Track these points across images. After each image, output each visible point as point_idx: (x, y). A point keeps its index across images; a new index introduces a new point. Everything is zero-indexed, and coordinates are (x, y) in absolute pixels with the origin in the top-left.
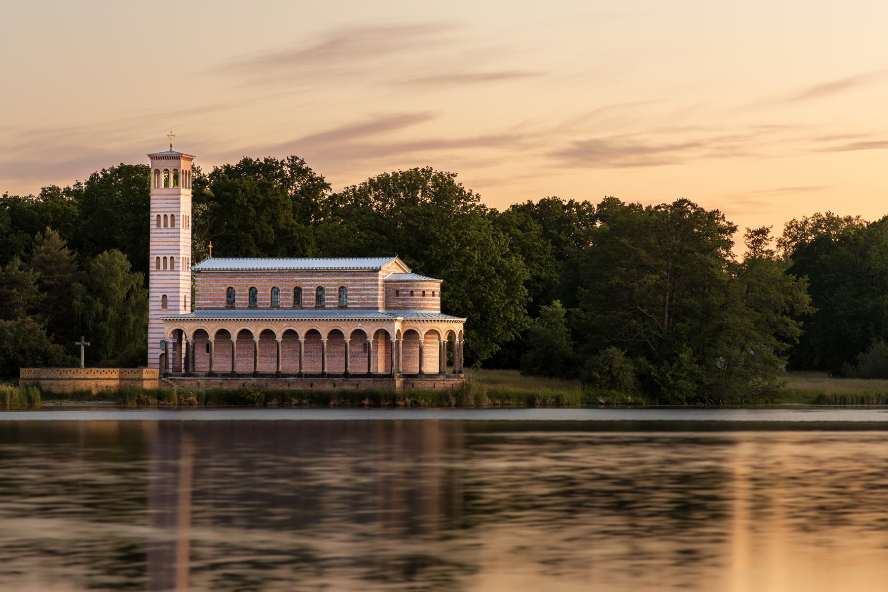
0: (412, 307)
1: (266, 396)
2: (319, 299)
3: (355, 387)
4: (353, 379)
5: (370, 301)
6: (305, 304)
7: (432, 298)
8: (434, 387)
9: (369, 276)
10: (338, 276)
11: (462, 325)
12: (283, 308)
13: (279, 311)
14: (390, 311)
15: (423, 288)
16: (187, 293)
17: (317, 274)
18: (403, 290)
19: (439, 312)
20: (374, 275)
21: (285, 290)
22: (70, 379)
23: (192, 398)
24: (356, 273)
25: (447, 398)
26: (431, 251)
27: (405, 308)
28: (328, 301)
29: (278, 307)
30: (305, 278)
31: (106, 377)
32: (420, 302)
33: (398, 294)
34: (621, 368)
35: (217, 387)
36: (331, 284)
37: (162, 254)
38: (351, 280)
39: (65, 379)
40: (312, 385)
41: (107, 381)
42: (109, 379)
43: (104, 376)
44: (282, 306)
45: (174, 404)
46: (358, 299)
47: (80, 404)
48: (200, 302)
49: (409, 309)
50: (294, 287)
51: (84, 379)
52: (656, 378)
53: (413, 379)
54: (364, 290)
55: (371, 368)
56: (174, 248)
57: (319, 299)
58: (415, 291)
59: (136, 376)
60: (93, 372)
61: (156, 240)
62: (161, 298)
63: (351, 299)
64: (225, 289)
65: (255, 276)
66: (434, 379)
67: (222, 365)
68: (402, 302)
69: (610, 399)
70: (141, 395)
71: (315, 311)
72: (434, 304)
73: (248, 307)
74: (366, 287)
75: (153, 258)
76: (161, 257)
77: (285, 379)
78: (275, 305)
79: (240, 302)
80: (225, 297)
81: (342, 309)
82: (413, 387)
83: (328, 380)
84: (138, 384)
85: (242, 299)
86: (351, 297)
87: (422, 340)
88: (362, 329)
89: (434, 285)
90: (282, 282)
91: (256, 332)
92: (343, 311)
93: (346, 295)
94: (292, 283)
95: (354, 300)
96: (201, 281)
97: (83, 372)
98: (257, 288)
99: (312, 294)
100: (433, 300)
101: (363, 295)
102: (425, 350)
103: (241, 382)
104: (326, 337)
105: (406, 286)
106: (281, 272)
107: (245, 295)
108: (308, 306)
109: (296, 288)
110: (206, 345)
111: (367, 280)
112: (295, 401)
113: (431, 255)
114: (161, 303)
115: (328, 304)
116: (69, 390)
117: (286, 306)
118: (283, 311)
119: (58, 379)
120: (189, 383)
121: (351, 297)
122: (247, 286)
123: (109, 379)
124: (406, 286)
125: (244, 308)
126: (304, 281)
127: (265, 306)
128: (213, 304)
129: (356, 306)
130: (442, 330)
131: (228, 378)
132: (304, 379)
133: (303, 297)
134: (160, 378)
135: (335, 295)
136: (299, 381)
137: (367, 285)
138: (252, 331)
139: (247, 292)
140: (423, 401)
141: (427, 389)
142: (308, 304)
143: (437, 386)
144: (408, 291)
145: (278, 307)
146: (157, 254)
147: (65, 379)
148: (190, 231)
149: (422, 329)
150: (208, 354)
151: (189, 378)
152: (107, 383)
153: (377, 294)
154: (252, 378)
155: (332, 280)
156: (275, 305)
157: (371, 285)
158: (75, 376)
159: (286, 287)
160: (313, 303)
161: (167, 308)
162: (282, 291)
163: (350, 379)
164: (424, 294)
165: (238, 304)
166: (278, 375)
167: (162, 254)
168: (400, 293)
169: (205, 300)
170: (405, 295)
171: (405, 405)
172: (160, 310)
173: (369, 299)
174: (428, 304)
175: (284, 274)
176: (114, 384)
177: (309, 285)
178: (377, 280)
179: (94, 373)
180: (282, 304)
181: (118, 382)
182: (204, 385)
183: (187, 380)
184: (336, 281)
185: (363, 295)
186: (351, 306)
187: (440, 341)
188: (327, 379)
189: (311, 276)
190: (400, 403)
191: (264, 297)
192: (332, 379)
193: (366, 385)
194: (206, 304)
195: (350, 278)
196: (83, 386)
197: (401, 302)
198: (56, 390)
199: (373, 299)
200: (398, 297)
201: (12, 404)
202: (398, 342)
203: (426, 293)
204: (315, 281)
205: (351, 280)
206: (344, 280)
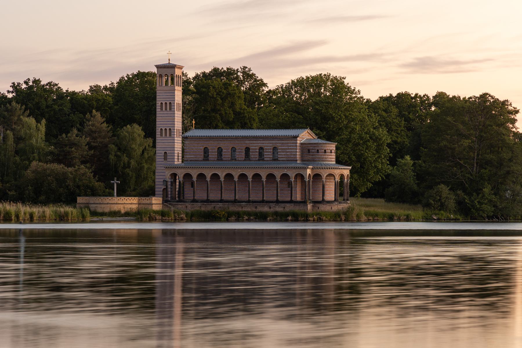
0: (318, 159)
1: (228, 214)
2: (261, 154)
3: (283, 209)
4: (282, 204)
5: (292, 156)
6: (252, 158)
7: (330, 154)
8: (332, 209)
9: (292, 140)
10: (273, 140)
11: (348, 171)
12: (239, 160)
13: (236, 162)
14: (304, 162)
15: (325, 148)
16: (179, 151)
17: (259, 139)
18: (313, 149)
19: (334, 163)
21: (239, 149)
22: (107, 204)
23: (182, 215)
24: (283, 139)
25: (339, 216)
26: (330, 125)
27: (314, 160)
28: (266, 156)
29: (235, 160)
30: (252, 142)
31: (130, 202)
32: (322, 157)
33: (310, 152)
34: (447, 198)
35: (198, 209)
36: (268, 146)
37: (164, 127)
38: (280, 143)
39: (105, 204)
40: (256, 207)
41: (130, 205)
42: (131, 204)
43: (129, 202)
44: (238, 159)
45: (172, 219)
46: (284, 155)
47: (114, 219)
48: (187, 156)
49: (316, 161)
50: (245, 147)
51: (116, 204)
52: (468, 204)
53: (318, 204)
54: (288, 149)
55: (293, 197)
56: (171, 123)
57: (261, 154)
58: (320, 150)
59: (148, 202)
60: (122, 199)
61: (160, 118)
62: (163, 154)
63: (280, 155)
64: (202, 148)
65: (221, 141)
66: (332, 204)
67: (201, 195)
68: (312, 157)
69: (440, 217)
70: (152, 213)
71: (258, 162)
72: (332, 158)
73: (217, 159)
74: (289, 148)
75: (158, 129)
76: (164, 129)
77: (239, 204)
78: (233, 159)
79: (212, 156)
80: (202, 153)
81: (275, 161)
82: (318, 209)
83: (266, 204)
84: (150, 207)
85: (213, 154)
86: (280, 153)
87: (324, 180)
88: (287, 173)
89: (332, 146)
90: (238, 144)
91: (222, 175)
92: (276, 162)
93: (277, 152)
95: (282, 155)
96: (188, 143)
97: (115, 199)
98: (222, 148)
99: (256, 152)
100: (331, 155)
101: (288, 152)
102: (326, 186)
103: (213, 206)
104: (265, 178)
105: (314, 147)
106: (237, 138)
107: (215, 152)
108: (254, 159)
109: (246, 148)
110: (190, 183)
111: (291, 143)
112: (246, 218)
113: (329, 128)
114: (163, 157)
115: (266, 158)
116: (107, 210)
117: (240, 159)
118: (238, 162)
119: (100, 204)
120: (181, 206)
121: (280, 153)
123: (131, 204)
124: (314, 147)
125: (214, 160)
126: (251, 144)
127: (227, 159)
128: (195, 157)
129: (283, 159)
130: (337, 174)
131: (205, 203)
132: (251, 204)
133: (251, 153)
134: (163, 203)
135: (270, 152)
136: (248, 205)
137: (291, 146)
138: (220, 175)
139: (216, 150)
140: (325, 217)
141: (327, 210)
142: (254, 158)
143: (333, 208)
144: (316, 150)
145: (235, 160)
146: (161, 127)
147: (105, 204)
148: (181, 113)
149: (324, 174)
150: (192, 188)
151: (181, 203)
152: (130, 206)
153: (297, 152)
154: (219, 203)
155: (269, 143)
156: (233, 159)
157: (293, 146)
158: (110, 202)
159: (241, 148)
160: (257, 157)
161: (167, 160)
162: (238, 150)
163: (279, 204)
164: (325, 152)
165: (211, 157)
166: (235, 201)
167: (164, 127)
168: (310, 151)
170: (314, 152)
171: (314, 220)
172: (163, 161)
173: (291, 155)
174: (327, 158)
175: (239, 139)
176: (135, 207)
177: (255, 146)
178: (297, 143)
179: (123, 200)
180: (238, 158)
181: (137, 206)
182: (190, 208)
183: (180, 204)
184: (271, 143)
185: (288, 152)
186: (280, 159)
187: (335, 180)
188: (266, 204)
189: (255, 141)
190: (310, 219)
191: (226, 154)
192: (269, 204)
193: (289, 208)
194: (191, 158)
195: (280, 142)
196: (116, 208)
197: (311, 157)
198: (99, 210)
199: (294, 155)
200: (309, 154)
201: (72, 219)
202: (309, 181)
203: (326, 151)
204: (258, 144)
205: (280, 143)
206: (276, 143)
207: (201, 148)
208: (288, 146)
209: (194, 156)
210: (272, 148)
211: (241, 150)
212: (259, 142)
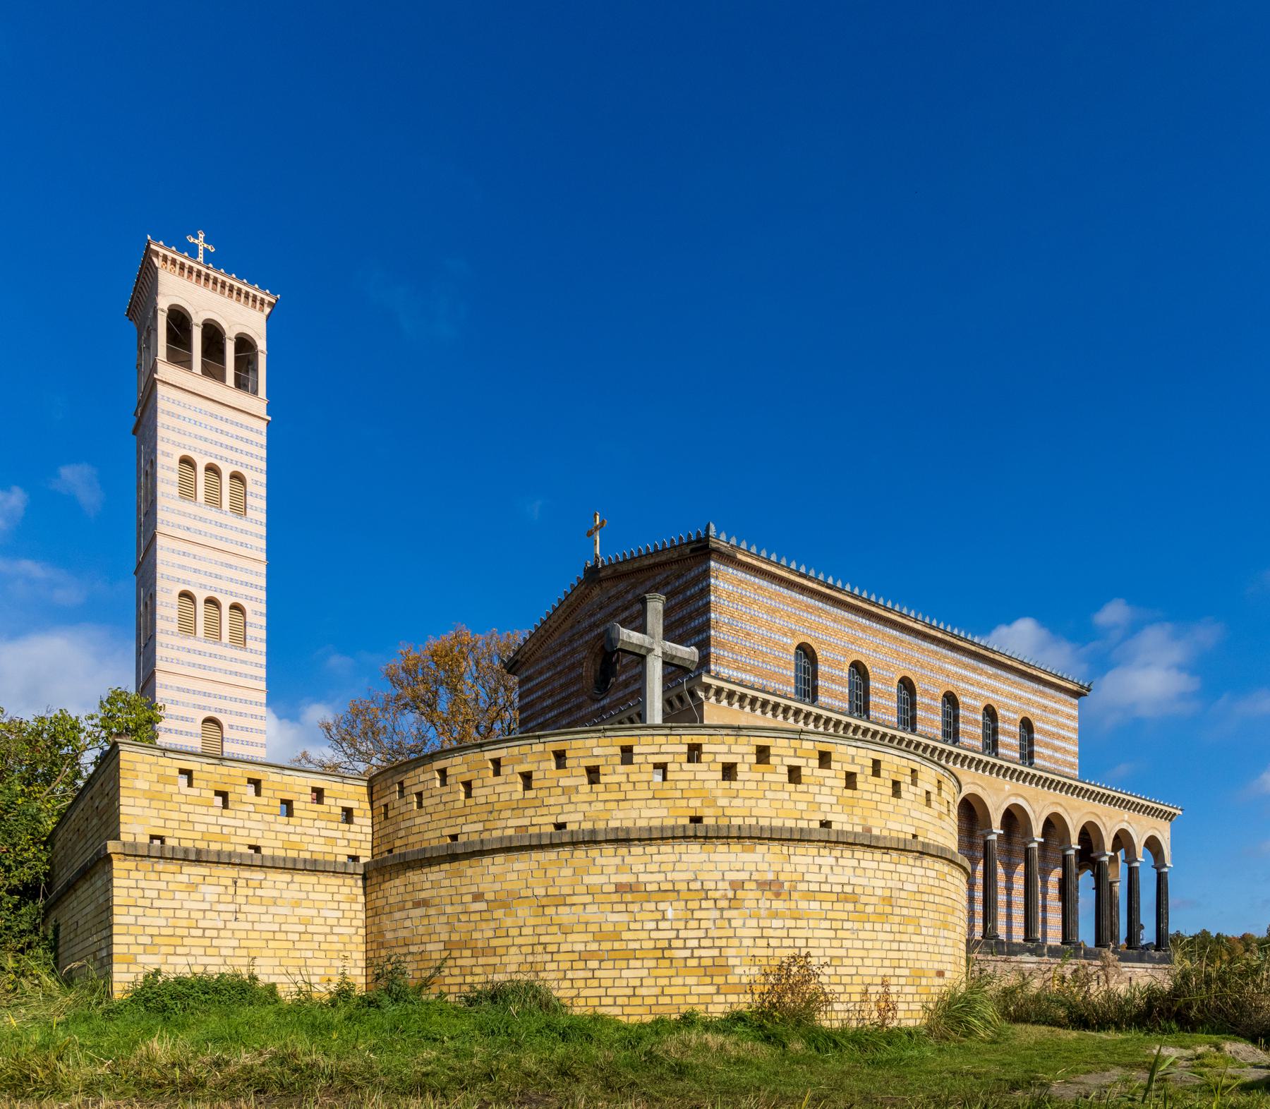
20: (1071, 704)
90: (922, 667)
94: (941, 678)
122: (846, 653)
169: (738, 669)
189: (974, 670)
207: (785, 639)
208: (1059, 725)
209: (756, 676)
210: (1018, 718)
211: (932, 699)
212: (984, 679)
